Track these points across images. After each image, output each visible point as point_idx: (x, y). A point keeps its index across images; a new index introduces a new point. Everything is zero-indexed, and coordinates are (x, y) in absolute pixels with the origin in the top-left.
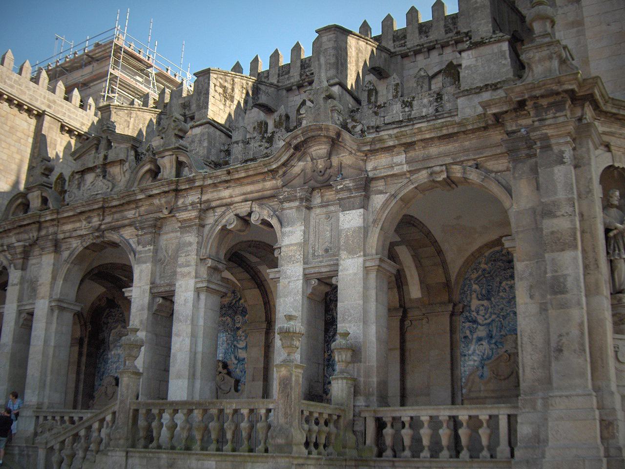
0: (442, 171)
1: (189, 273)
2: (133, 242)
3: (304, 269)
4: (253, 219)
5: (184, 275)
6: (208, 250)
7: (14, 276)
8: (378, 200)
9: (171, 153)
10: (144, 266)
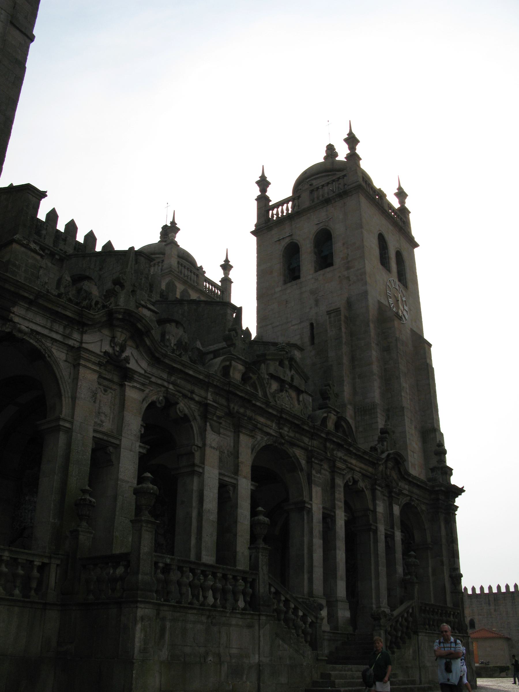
2: (303, 462)
4: (359, 484)
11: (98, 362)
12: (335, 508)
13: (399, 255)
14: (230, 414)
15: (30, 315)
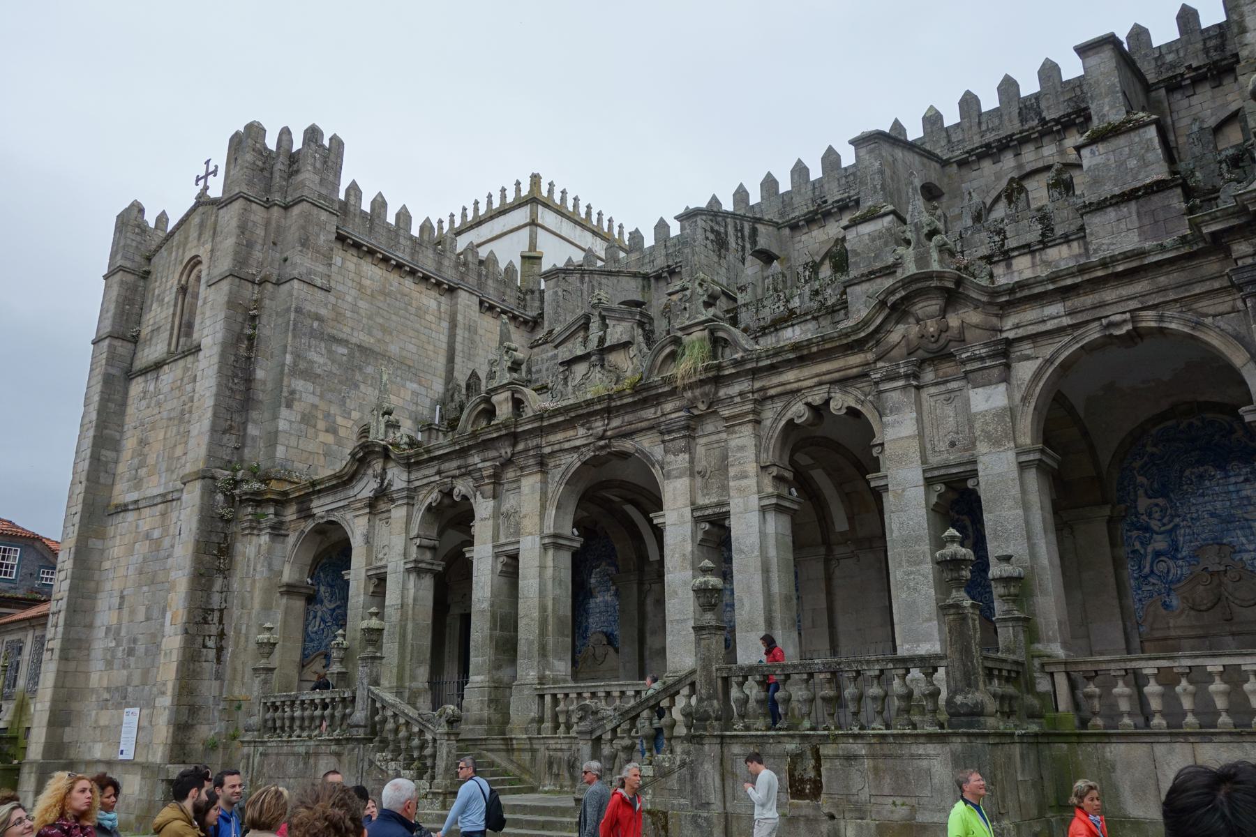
0: (1125, 321)
2: (658, 452)
3: (924, 471)
4: (832, 404)
5: (739, 490)
6: (771, 453)
7: (483, 508)
8: (1024, 371)
9: (701, 328)
15: (322, 501)
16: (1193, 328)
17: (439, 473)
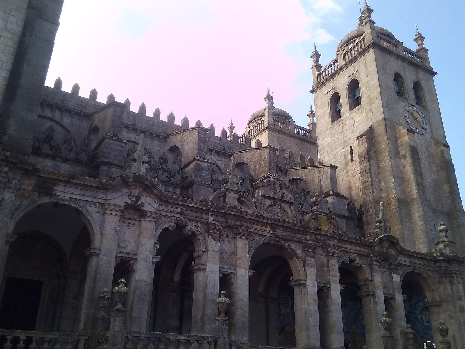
1: (337, 281)
2: (299, 252)
4: (356, 262)
9: (324, 215)
10: (312, 269)
11: (118, 210)
12: (330, 282)
13: (417, 86)
14: (229, 227)
15: (68, 189)
16: (427, 277)
17: (181, 213)
